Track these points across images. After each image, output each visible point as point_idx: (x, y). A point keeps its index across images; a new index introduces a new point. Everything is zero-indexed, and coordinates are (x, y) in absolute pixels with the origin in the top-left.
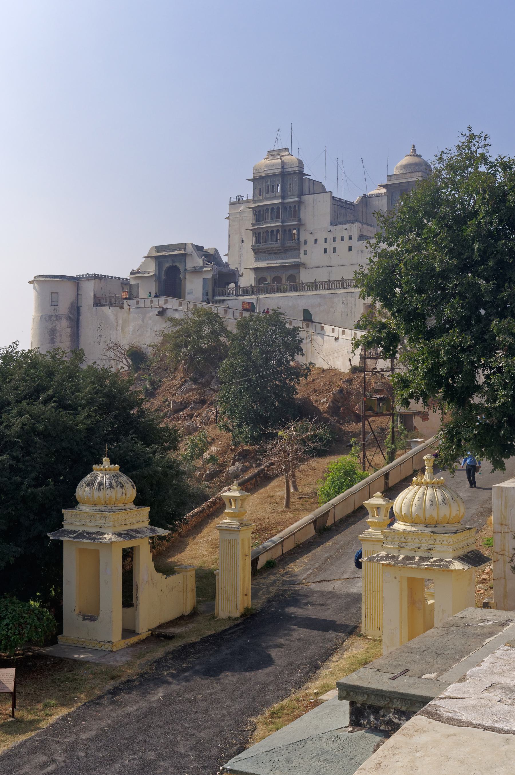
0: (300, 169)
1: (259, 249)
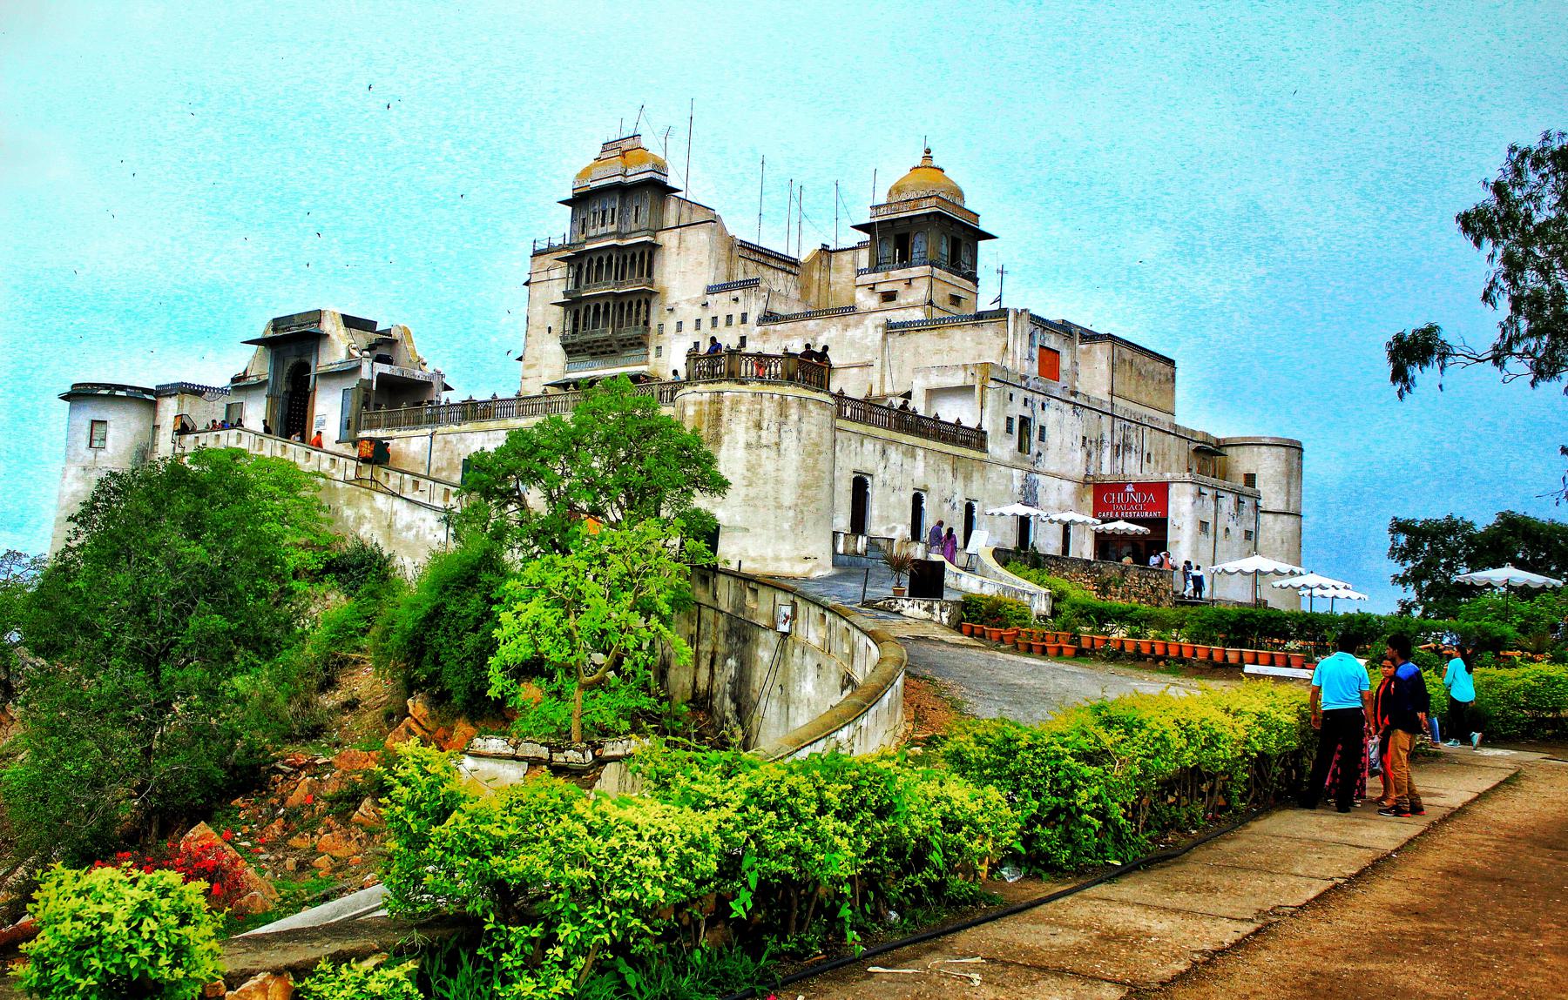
0: (657, 176)
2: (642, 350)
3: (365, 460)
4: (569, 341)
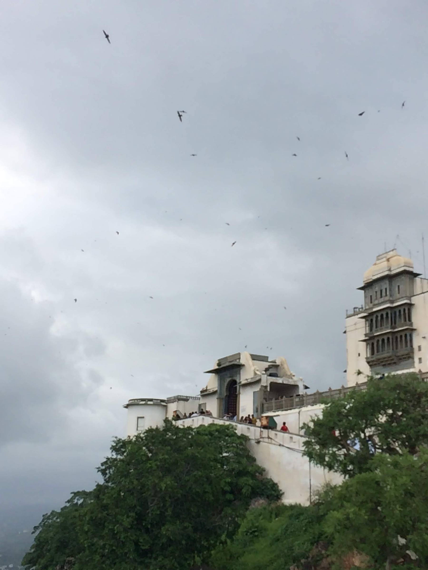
0: (408, 269)
1: (373, 361)
2: (411, 360)
3: (265, 427)
4: (369, 360)
